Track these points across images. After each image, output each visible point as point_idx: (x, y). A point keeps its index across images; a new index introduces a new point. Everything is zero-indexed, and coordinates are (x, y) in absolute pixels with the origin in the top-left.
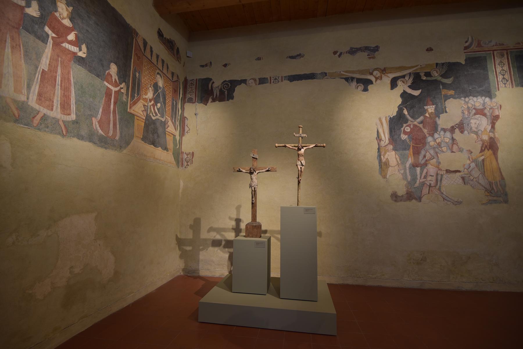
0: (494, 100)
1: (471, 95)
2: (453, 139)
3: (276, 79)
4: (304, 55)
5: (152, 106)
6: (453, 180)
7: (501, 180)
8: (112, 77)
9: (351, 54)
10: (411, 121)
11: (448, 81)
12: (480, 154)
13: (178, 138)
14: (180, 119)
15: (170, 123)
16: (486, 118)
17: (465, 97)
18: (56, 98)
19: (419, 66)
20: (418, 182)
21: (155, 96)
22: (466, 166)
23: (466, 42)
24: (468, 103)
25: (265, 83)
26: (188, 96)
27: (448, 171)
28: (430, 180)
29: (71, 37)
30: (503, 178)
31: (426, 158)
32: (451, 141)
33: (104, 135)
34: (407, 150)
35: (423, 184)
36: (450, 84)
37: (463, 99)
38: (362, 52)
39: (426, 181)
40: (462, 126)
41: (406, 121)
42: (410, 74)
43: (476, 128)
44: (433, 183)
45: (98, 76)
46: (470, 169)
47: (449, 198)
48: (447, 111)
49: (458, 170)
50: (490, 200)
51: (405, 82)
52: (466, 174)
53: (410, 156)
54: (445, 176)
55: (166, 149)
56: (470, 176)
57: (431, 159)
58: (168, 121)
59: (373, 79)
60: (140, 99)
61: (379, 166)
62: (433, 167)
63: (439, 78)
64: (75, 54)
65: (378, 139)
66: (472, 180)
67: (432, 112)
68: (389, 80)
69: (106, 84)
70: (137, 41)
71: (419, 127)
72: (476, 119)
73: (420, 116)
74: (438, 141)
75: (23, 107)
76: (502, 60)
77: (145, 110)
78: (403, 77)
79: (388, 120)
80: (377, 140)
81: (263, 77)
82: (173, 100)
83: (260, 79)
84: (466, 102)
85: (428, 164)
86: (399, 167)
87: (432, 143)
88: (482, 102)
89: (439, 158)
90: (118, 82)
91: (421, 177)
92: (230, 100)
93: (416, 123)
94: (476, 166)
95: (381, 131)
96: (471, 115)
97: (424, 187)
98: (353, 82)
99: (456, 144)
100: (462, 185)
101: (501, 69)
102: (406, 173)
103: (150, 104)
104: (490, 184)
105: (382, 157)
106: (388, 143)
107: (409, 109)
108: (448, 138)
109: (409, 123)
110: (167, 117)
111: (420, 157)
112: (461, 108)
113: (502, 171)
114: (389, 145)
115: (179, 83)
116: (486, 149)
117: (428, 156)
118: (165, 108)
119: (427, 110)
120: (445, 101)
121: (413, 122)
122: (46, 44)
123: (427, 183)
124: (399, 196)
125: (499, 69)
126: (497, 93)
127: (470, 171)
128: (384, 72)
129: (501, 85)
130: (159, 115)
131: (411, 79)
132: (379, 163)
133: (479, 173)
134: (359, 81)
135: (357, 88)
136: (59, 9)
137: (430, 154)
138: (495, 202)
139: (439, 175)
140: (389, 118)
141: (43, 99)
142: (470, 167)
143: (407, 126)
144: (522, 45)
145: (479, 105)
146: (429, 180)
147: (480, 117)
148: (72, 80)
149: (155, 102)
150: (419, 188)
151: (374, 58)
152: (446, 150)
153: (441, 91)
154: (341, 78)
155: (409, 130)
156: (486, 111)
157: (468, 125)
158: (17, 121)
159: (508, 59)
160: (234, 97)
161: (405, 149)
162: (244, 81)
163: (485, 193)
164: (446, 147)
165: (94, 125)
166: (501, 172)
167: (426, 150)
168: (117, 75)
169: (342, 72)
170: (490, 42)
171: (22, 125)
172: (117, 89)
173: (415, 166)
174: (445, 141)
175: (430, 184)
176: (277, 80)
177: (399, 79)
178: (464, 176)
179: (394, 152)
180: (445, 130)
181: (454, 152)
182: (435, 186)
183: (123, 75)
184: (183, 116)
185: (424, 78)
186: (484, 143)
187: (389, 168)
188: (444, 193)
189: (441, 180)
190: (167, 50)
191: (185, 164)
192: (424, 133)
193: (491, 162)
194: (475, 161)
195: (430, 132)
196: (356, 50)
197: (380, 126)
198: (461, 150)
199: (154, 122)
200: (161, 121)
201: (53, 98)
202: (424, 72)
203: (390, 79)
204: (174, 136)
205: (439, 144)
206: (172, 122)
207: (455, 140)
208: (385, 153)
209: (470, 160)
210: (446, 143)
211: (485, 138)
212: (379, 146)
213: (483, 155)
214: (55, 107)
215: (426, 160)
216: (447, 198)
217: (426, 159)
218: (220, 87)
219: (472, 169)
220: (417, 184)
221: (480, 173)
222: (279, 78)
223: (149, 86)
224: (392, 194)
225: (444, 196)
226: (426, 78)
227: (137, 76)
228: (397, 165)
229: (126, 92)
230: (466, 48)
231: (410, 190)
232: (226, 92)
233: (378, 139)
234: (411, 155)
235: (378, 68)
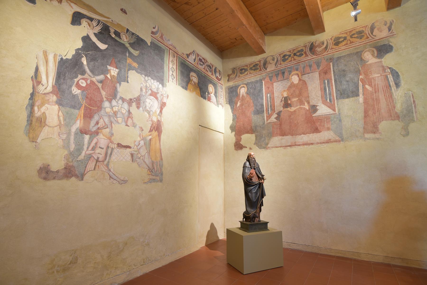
0: (164, 88)
1: (150, 76)
6: (123, 156)
7: (160, 160)
10: (89, 75)
12: (149, 133)
16: (157, 102)
19: (111, 20)
22: (137, 143)
23: (154, 28)
24: (146, 81)
27: (120, 145)
28: (98, 153)
30: (162, 159)
31: (99, 125)
32: (127, 114)
35: (89, 157)
36: (136, 57)
37: (143, 76)
39: (94, 153)
40: (139, 101)
41: (83, 72)
42: (99, 21)
43: (150, 108)
44: (101, 157)
48: (129, 81)
50: (150, 179)
52: (135, 151)
53: (79, 117)
54: (115, 151)
56: (138, 154)
57: (105, 128)
61: (27, 121)
62: (105, 138)
63: (127, 45)
65: (34, 79)
66: (139, 158)
67: (114, 75)
68: (71, 11)
71: (98, 86)
73: (101, 75)
74: (114, 110)
76: (173, 60)
78: (91, 19)
79: (57, 61)
80: (32, 80)
85: (99, 134)
86: (60, 130)
87: (108, 110)
88: (157, 86)
89: (113, 129)
91: (88, 148)
93: (94, 79)
94: (145, 144)
95: (42, 69)
97: (89, 162)
99: (132, 118)
100: (131, 162)
101: (172, 66)
104: (153, 163)
105: (36, 108)
106: (51, 90)
109: (86, 76)
111: (92, 122)
113: (162, 152)
114: (51, 95)
116: (154, 130)
117: (101, 124)
120: (128, 70)
121: (92, 77)
125: (171, 66)
126: (167, 84)
127: (138, 149)
129: (170, 79)
132: (27, 117)
133: (146, 153)
138: (154, 180)
139: (110, 148)
142: (140, 144)
143: (83, 79)
144: (185, 56)
145: (154, 88)
146: (98, 152)
147: (153, 99)
150: (84, 162)
152: (121, 121)
155: (84, 85)
156: (158, 96)
157: (144, 103)
159: (177, 61)
161: (74, 107)
163: (148, 171)
164: (121, 118)
166: (161, 153)
167: (100, 115)
170: (169, 40)
173: (83, 132)
174: (121, 112)
175: (98, 158)
178: (133, 152)
179: (56, 107)
180: (123, 100)
181: (128, 126)
182: (103, 161)
185: (113, 36)
186: (153, 124)
187: (44, 128)
188: (112, 170)
189: (111, 154)
193: (156, 143)
194: (144, 139)
195: (108, 96)
197: (43, 63)
205: (115, 113)
207: (131, 113)
208: (42, 104)
209: (140, 137)
210: (123, 114)
211: (155, 119)
212: (33, 91)
213: (151, 135)
215: (98, 128)
217: (99, 127)
219: (141, 147)
220: (82, 157)
224: (41, 168)
225: (111, 173)
228: (58, 127)
230: (153, 33)
231: (71, 164)
233: (34, 79)
234: (81, 117)
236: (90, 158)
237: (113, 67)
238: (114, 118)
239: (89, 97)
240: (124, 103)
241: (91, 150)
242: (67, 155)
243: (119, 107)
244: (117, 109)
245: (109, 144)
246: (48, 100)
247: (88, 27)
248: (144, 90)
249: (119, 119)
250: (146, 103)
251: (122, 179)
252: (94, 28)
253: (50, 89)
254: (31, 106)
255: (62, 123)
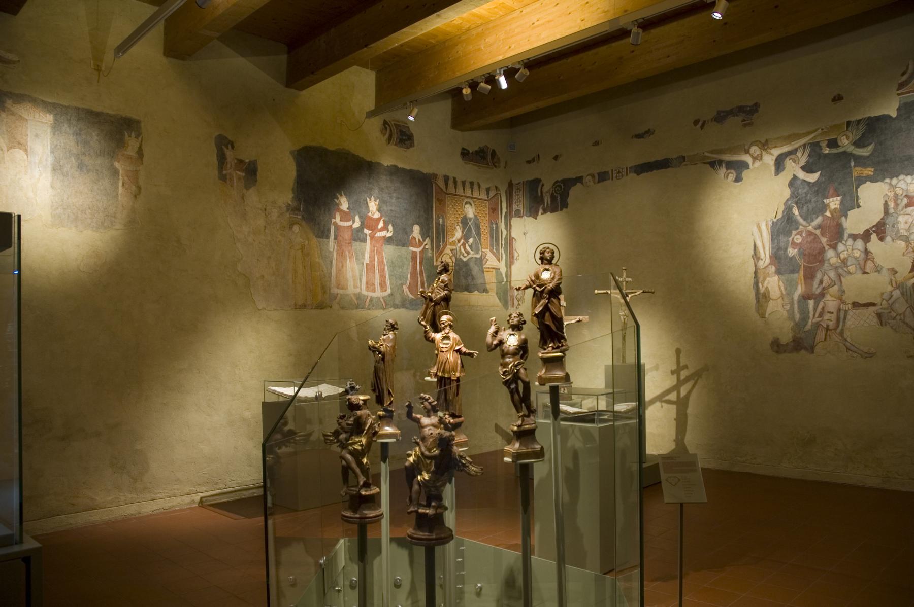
2: (867, 252)
3: (619, 172)
4: (654, 131)
5: (462, 247)
8: (415, 239)
9: (718, 122)
10: (804, 226)
11: (863, 152)
13: (503, 270)
14: (506, 243)
15: (490, 255)
17: (891, 178)
18: (376, 281)
19: (820, 130)
20: (810, 323)
21: (465, 233)
22: (885, 296)
25: (606, 180)
26: (515, 207)
27: (855, 305)
28: (828, 320)
29: (381, 225)
31: (824, 285)
32: (863, 255)
33: (414, 298)
34: (795, 273)
35: (817, 325)
36: (868, 157)
37: (887, 180)
38: (734, 116)
40: (882, 228)
42: (804, 145)
43: (908, 230)
44: (832, 324)
45: (403, 245)
46: (892, 300)
47: (856, 347)
48: (861, 204)
49: (871, 303)
51: (797, 162)
53: (799, 282)
54: (850, 313)
55: (486, 290)
56: (890, 312)
58: (486, 254)
59: (748, 159)
60: (446, 246)
61: (756, 299)
63: (851, 149)
64: (384, 237)
67: (835, 209)
69: (411, 248)
70: (437, 184)
71: (816, 235)
72: (907, 214)
74: (842, 256)
75: (359, 296)
77: (454, 255)
79: (770, 227)
80: (753, 259)
81: (603, 171)
82: (492, 223)
83: (599, 174)
84: (893, 186)
85: (826, 294)
87: (834, 260)
89: (843, 284)
90: (422, 241)
91: (814, 315)
92: (564, 210)
93: (810, 228)
94: (902, 294)
95: (759, 244)
96: (900, 208)
97: (818, 331)
98: (721, 169)
99: (872, 259)
100: (878, 326)
102: (793, 309)
103: (459, 245)
105: (760, 285)
106: (769, 262)
107: (801, 206)
108: (859, 250)
110: (483, 250)
112: (884, 197)
114: (770, 266)
115: (499, 196)
118: (480, 240)
119: (827, 206)
120: (856, 190)
122: (366, 242)
123: (823, 324)
124: (782, 345)
127: (890, 304)
128: (766, 147)
130: (472, 252)
131: (806, 155)
133: (906, 307)
134: (730, 165)
135: (727, 178)
136: (371, 209)
137: (829, 277)
140: (772, 222)
141: (369, 286)
143: (797, 234)
148: (385, 261)
149: (465, 239)
151: (750, 124)
152: (854, 269)
153: (851, 170)
154: (705, 163)
157: (893, 226)
158: (357, 308)
160: (568, 204)
162: (579, 179)
164: (854, 266)
165: (405, 292)
167: (823, 271)
168: (420, 234)
169: (706, 154)
171: (360, 310)
172: (421, 249)
175: (828, 326)
176: (620, 174)
177: (787, 156)
178: (880, 311)
179: (776, 278)
180: (854, 237)
181: (867, 273)
182: (835, 329)
183: (425, 233)
184: (510, 236)
185: (827, 151)
188: (849, 339)
190: (476, 165)
191: (516, 303)
192: (823, 245)
195: (831, 242)
196: (725, 114)
198: (879, 269)
199: (466, 264)
200: (476, 258)
201: (375, 282)
202: (828, 140)
203: (774, 158)
204: (497, 269)
206: (493, 253)
208: (765, 279)
209: (892, 285)
210: (856, 258)
214: (376, 288)
216: (852, 348)
218: (551, 192)
219: (896, 300)
221: (908, 306)
222: (623, 170)
223: (456, 224)
226: (829, 151)
227: (441, 222)
228: (781, 298)
229: (430, 246)
231: (799, 335)
232: (559, 198)
235: (757, 141)
236: (818, 326)
237: (832, 197)
238: (843, 269)
239: (807, 253)
240: (855, 242)
241: (818, 317)
242: (793, 326)
243: (849, 250)
244: (847, 254)
245: (840, 306)
246: (768, 273)
247: (793, 164)
248: (891, 205)
249: (850, 268)
250: (899, 225)
251: (866, 350)
252: (800, 160)
253: (768, 261)
254: (756, 284)
255: (784, 293)
